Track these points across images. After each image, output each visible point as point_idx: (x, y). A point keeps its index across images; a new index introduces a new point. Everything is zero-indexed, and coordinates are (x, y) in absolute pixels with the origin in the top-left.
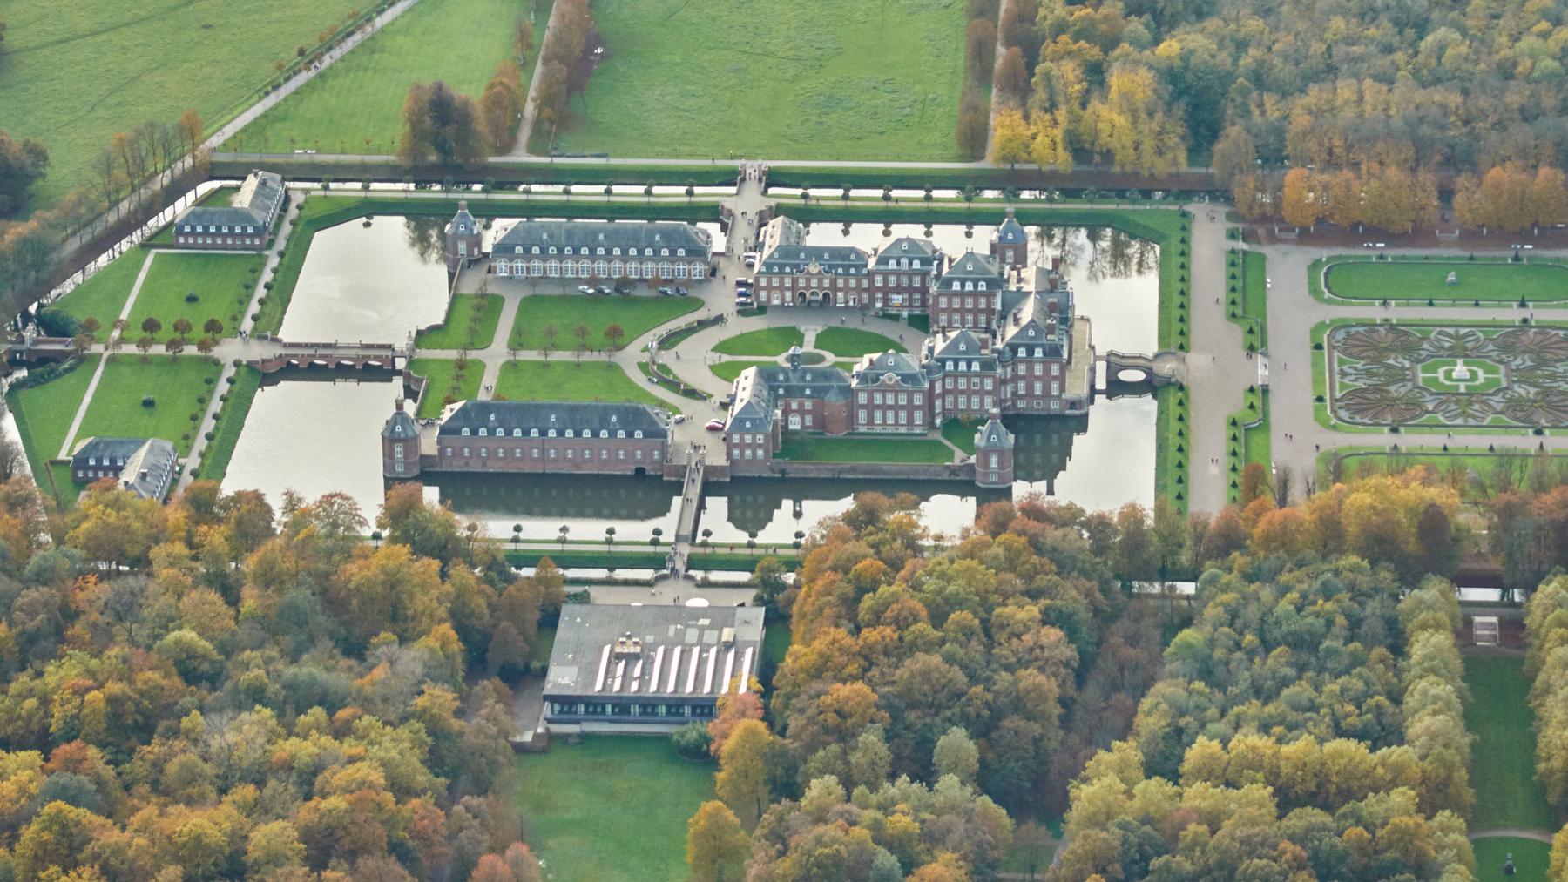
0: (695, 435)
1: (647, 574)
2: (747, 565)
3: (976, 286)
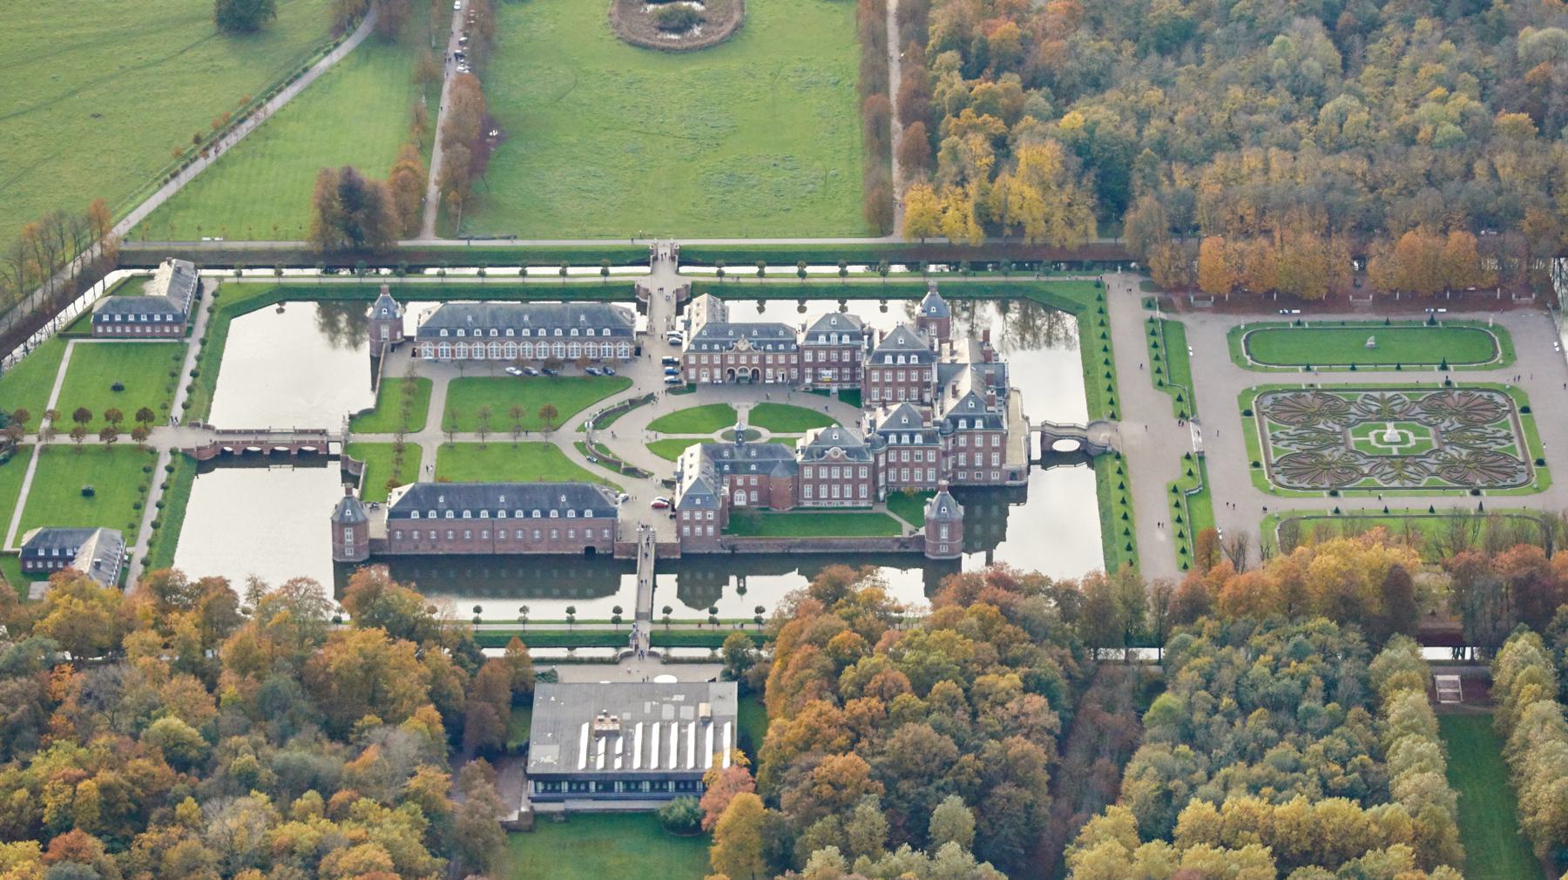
0: (641, 514)
1: (608, 652)
2: (713, 641)
3: (908, 359)
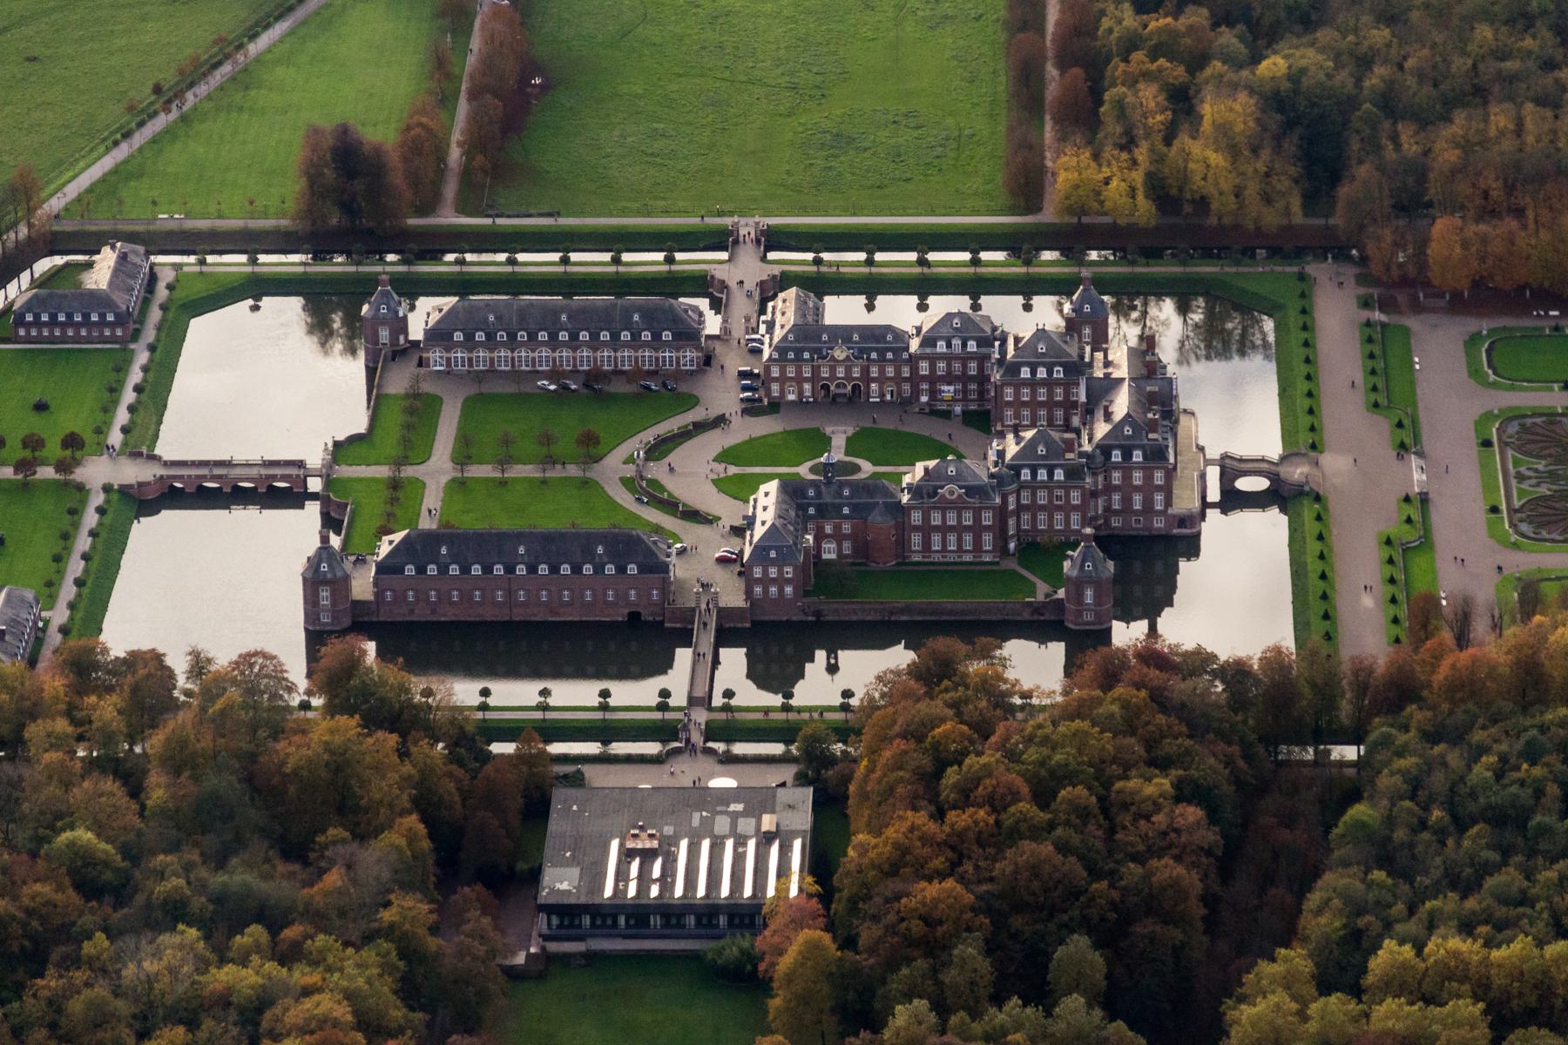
0: (702, 567)
1: (652, 748)
2: (783, 733)
